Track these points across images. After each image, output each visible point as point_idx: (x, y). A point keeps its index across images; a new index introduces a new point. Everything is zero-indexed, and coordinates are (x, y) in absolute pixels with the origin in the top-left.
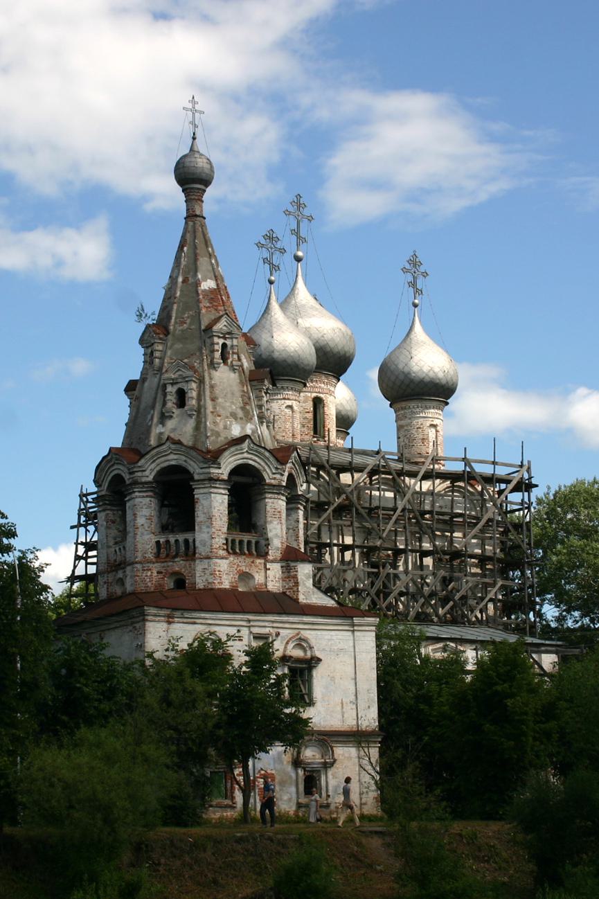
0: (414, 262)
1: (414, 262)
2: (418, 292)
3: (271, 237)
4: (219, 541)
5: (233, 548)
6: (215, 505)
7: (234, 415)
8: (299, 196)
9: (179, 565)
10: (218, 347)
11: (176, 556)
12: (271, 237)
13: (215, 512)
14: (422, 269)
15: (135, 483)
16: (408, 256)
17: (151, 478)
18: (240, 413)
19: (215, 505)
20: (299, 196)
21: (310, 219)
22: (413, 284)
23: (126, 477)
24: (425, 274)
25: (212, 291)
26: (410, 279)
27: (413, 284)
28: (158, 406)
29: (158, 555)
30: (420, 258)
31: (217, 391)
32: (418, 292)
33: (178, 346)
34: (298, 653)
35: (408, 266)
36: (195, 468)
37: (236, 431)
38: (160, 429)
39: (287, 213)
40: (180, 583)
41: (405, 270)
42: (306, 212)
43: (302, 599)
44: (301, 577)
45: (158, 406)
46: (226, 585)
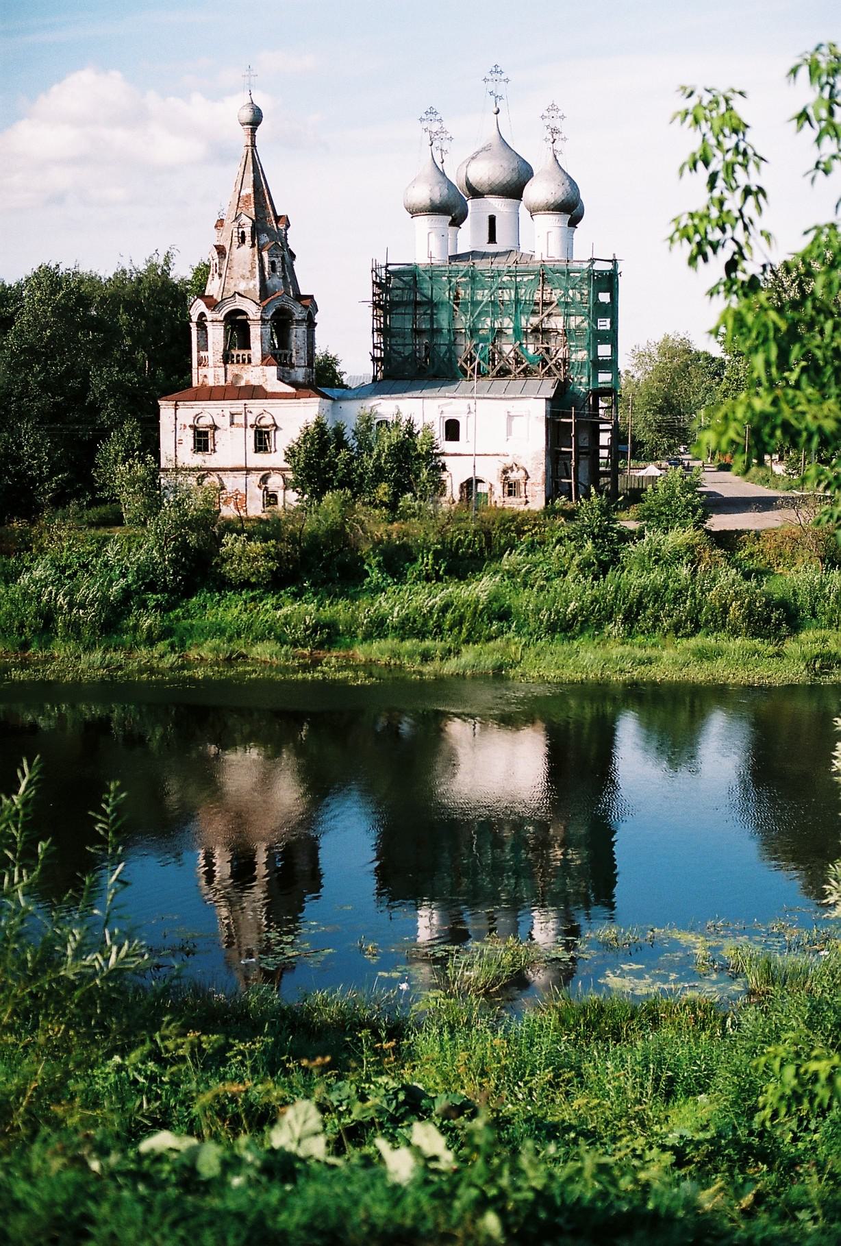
7: (243, 277)
18: (248, 274)
37: (242, 287)
43: (269, 389)
46: (222, 383)
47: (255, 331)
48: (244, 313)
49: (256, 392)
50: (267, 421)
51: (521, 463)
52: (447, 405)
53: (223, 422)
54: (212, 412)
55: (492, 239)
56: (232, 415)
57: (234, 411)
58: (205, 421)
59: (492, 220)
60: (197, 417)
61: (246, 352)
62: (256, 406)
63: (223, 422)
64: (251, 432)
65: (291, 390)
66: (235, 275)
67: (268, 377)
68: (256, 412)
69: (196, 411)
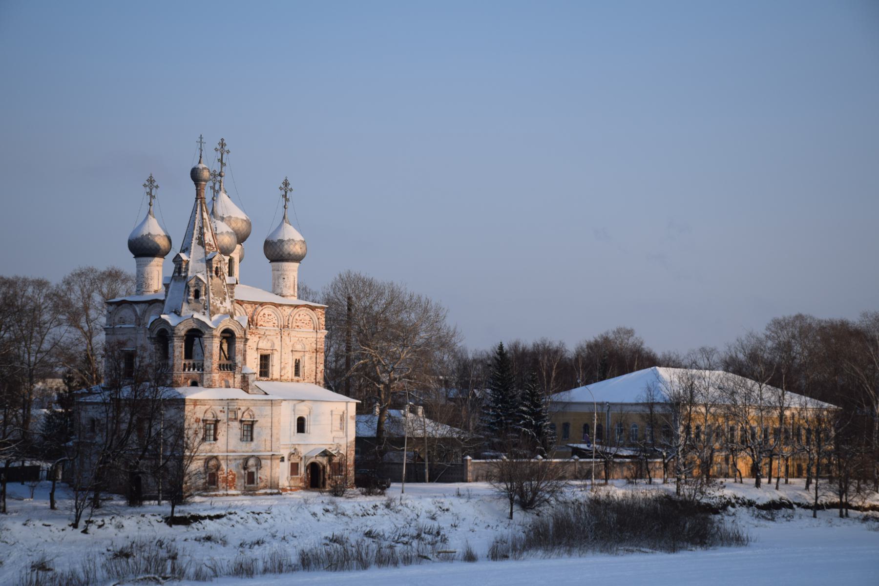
0: (286, 184)
1: (286, 184)
2: (287, 200)
4: (216, 365)
5: (221, 367)
8: (222, 140)
10: (214, 269)
13: (214, 352)
20: (222, 140)
21: (228, 152)
22: (285, 196)
26: (284, 193)
27: (285, 196)
30: (289, 181)
32: (287, 200)
34: (247, 417)
39: (216, 150)
41: (281, 188)
42: (226, 148)
44: (250, 381)
58: (209, 417)
59: (231, 261)
68: (243, 409)
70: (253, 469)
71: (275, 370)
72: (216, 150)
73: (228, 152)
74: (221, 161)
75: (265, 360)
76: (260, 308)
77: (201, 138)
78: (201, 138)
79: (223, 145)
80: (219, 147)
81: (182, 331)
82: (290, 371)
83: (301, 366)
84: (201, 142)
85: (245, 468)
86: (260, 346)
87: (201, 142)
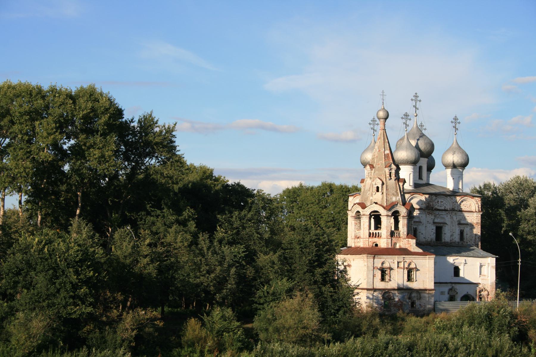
0: (456, 119)
1: (456, 119)
3: (406, 115)
6: (387, 222)
7: (393, 194)
8: (416, 94)
9: (376, 240)
11: (375, 237)
12: (406, 115)
14: (458, 121)
15: (364, 215)
16: (453, 116)
17: (368, 214)
18: (395, 193)
19: (387, 222)
21: (420, 101)
22: (455, 127)
23: (362, 213)
24: (459, 123)
25: (388, 154)
28: (371, 190)
29: (370, 236)
31: (389, 187)
33: (377, 172)
35: (453, 121)
36: (383, 212)
37: (394, 199)
38: (371, 198)
39: (412, 100)
40: (376, 245)
41: (452, 122)
42: (419, 99)
43: (412, 250)
45: (371, 190)
46: (390, 247)
47: (384, 220)
48: (378, 212)
49: (404, 252)
50: (413, 266)
51: (486, 288)
52: (457, 259)
53: (395, 266)
54: (390, 261)
55: (420, 178)
56: (398, 263)
57: (399, 260)
60: (383, 263)
61: (380, 231)
62: (408, 259)
63: (395, 266)
64: (406, 271)
65: (420, 251)
66: (390, 193)
67: (411, 244)
68: (408, 261)
69: (382, 260)
70: (415, 299)
71: (447, 237)
72: (412, 100)
73: (420, 101)
74: (415, 106)
75: (439, 230)
76: (435, 198)
77: (383, 92)
78: (383, 92)
79: (416, 96)
80: (413, 98)
81: (368, 211)
82: (457, 238)
83: (465, 234)
84: (383, 95)
85: (409, 298)
86: (436, 221)
87: (383, 95)
